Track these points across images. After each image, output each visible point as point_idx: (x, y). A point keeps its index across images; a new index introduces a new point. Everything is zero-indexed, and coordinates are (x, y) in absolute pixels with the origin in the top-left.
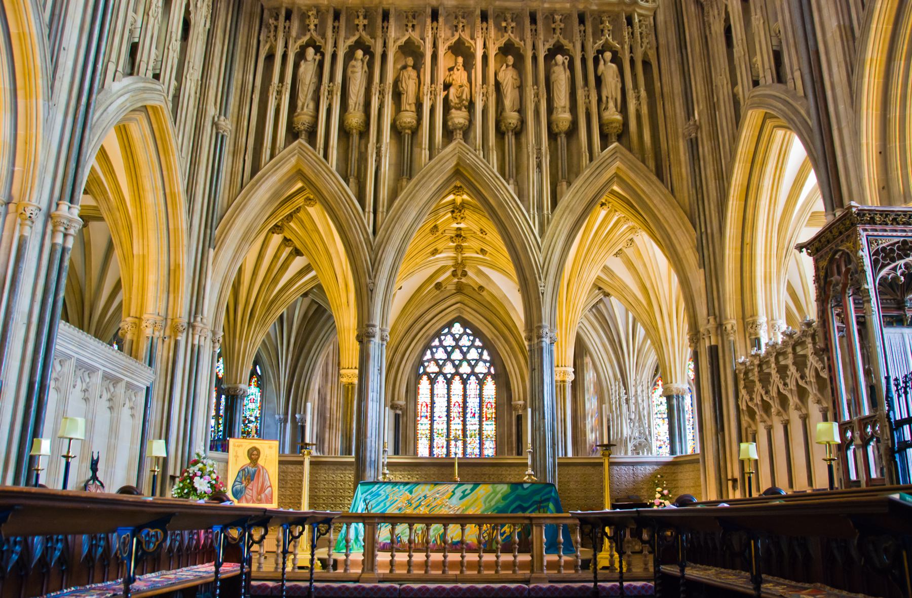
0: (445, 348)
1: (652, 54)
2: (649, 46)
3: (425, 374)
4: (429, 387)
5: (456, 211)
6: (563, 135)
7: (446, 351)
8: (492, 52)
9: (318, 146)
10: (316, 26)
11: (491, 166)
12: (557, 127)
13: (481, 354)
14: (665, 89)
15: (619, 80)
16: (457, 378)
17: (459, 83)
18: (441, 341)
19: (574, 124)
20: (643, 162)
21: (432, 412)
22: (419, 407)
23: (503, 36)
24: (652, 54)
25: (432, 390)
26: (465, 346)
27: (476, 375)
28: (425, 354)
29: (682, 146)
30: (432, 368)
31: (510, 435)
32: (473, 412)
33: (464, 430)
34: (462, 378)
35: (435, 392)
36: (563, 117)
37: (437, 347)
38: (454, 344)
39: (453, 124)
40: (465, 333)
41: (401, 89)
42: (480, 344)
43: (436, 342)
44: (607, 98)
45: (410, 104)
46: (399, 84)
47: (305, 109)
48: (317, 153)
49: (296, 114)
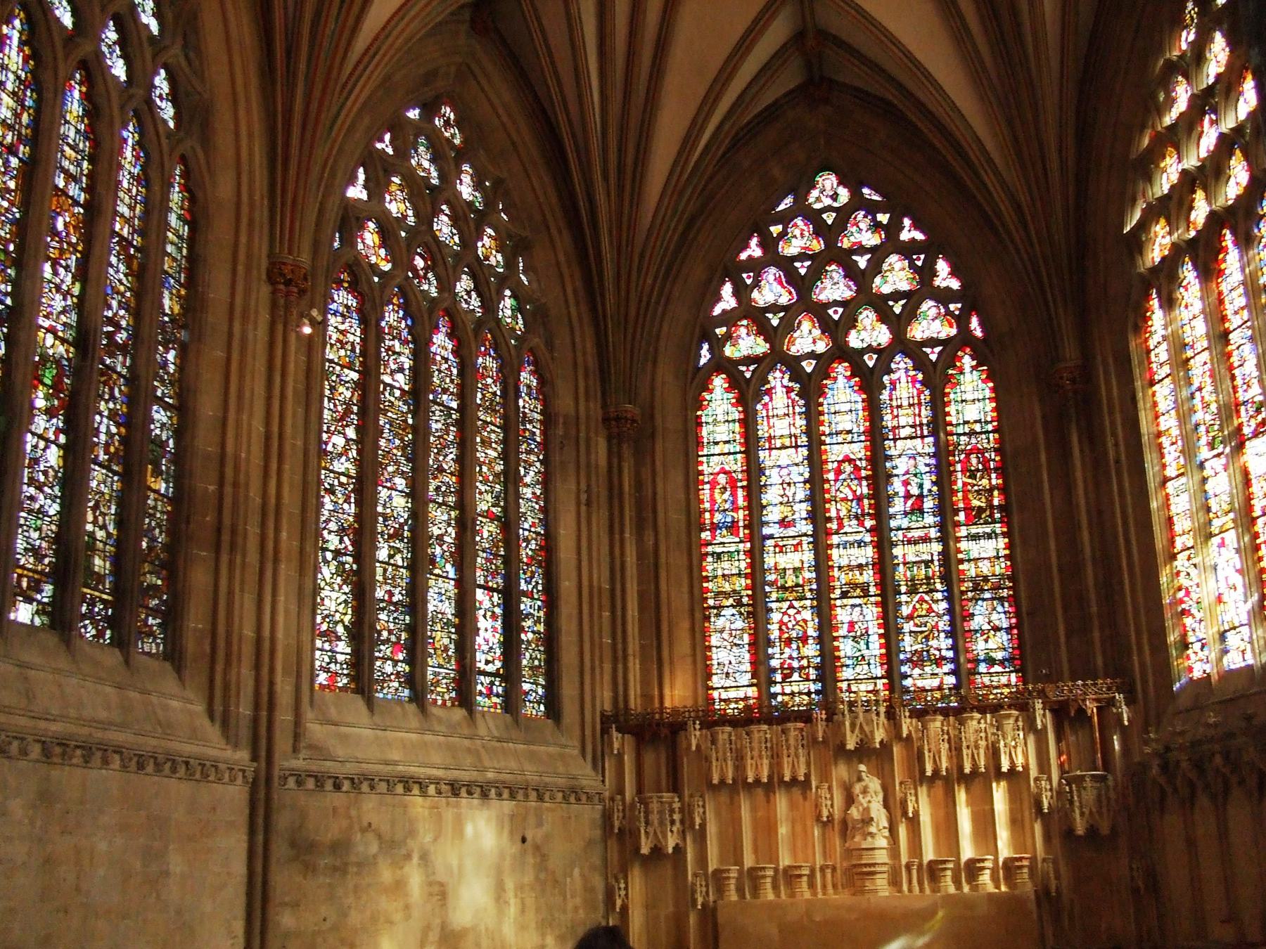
0: (786, 265)
3: (719, 371)
4: (736, 414)
7: (792, 278)
13: (925, 274)
16: (842, 369)
18: (769, 244)
21: (755, 508)
22: (705, 493)
25: (748, 424)
26: (861, 249)
27: (914, 350)
28: (719, 298)
30: (747, 344)
31: (1072, 570)
32: (914, 491)
33: (883, 564)
34: (858, 369)
35: (763, 430)
37: (756, 267)
38: (817, 246)
40: (857, 202)
42: (919, 236)
43: (754, 250)
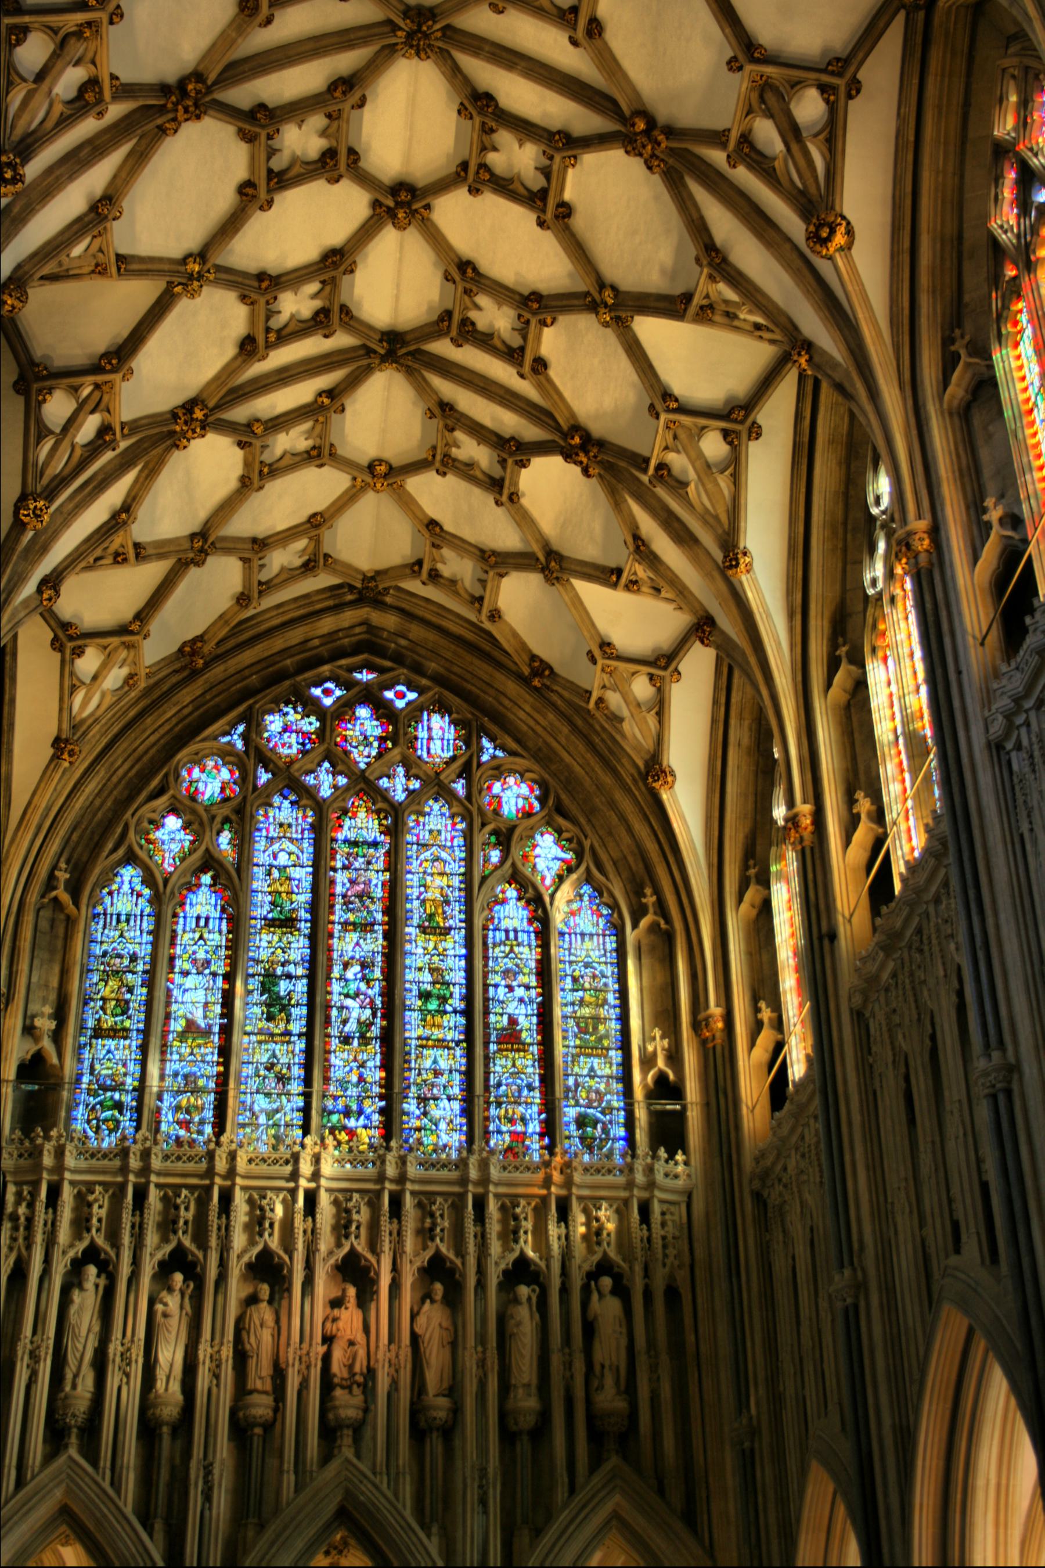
1: (682, 1276)
2: (677, 1263)
5: (334, 1552)
6: (525, 1438)
8: (408, 1279)
9: (102, 1464)
10: (100, 1220)
11: (400, 1506)
12: (516, 1423)
14: (703, 1348)
15: (624, 1330)
17: (348, 1335)
19: (545, 1415)
20: (661, 1491)
23: (425, 1248)
24: (682, 1276)
29: (729, 1460)
36: (527, 1403)
39: (337, 1418)
41: (248, 1347)
44: (603, 1366)
45: (261, 1378)
46: (244, 1334)
47: (79, 1388)
48: (99, 1479)
49: (62, 1395)
